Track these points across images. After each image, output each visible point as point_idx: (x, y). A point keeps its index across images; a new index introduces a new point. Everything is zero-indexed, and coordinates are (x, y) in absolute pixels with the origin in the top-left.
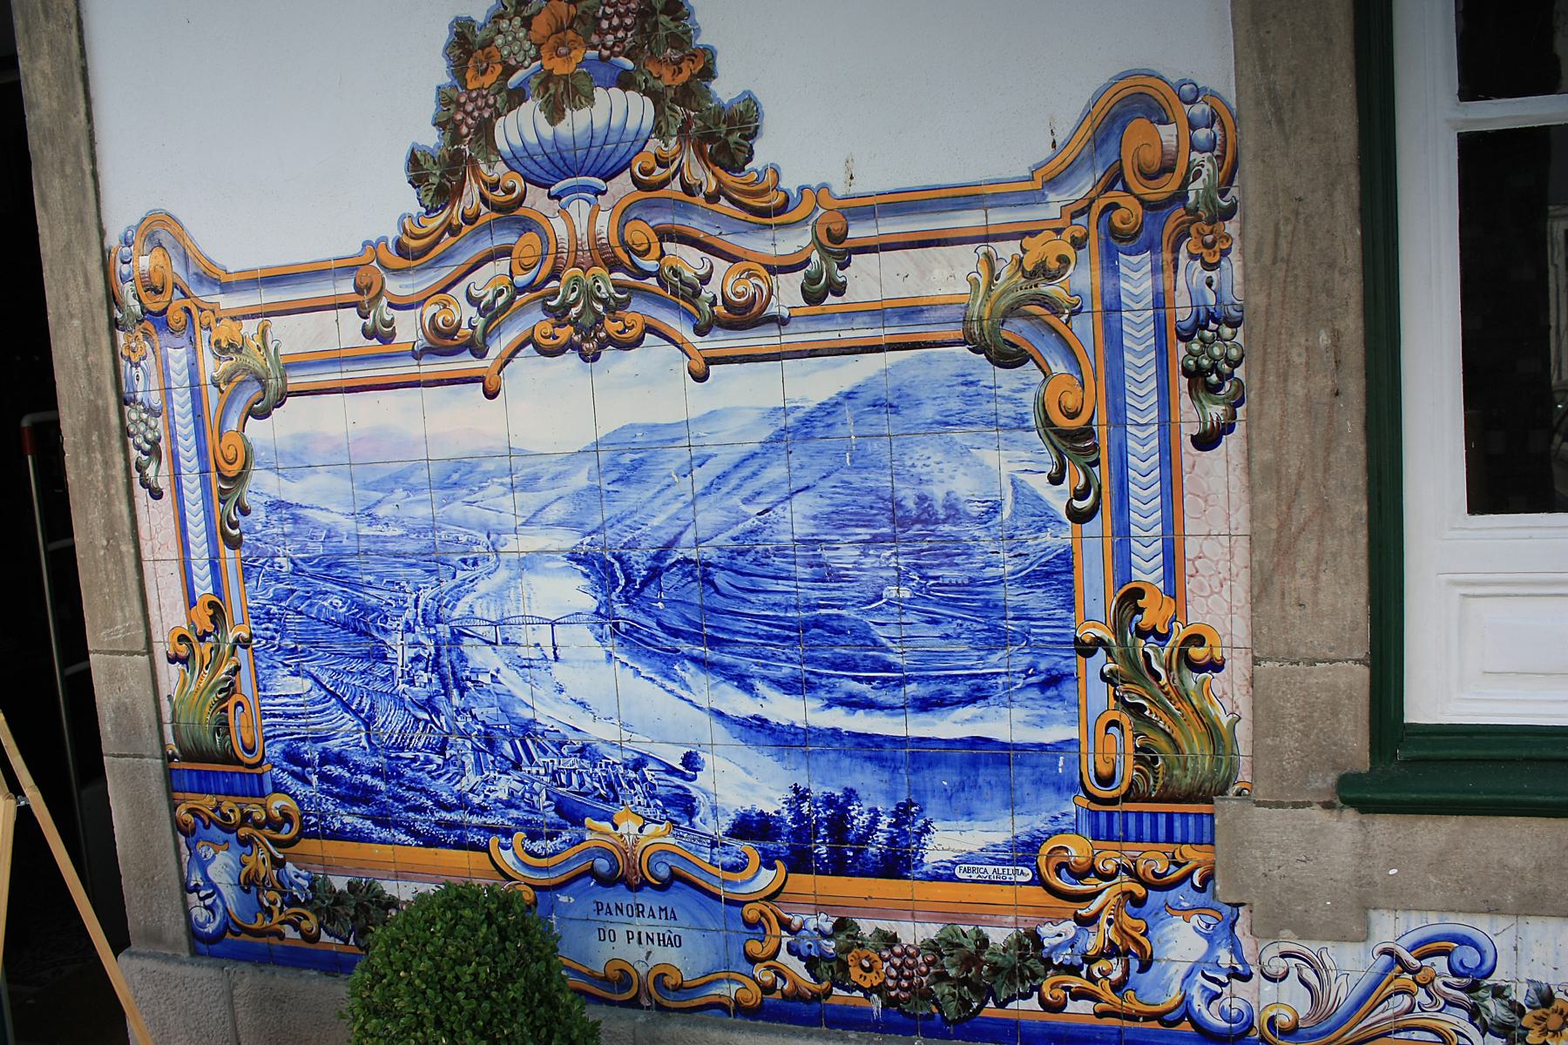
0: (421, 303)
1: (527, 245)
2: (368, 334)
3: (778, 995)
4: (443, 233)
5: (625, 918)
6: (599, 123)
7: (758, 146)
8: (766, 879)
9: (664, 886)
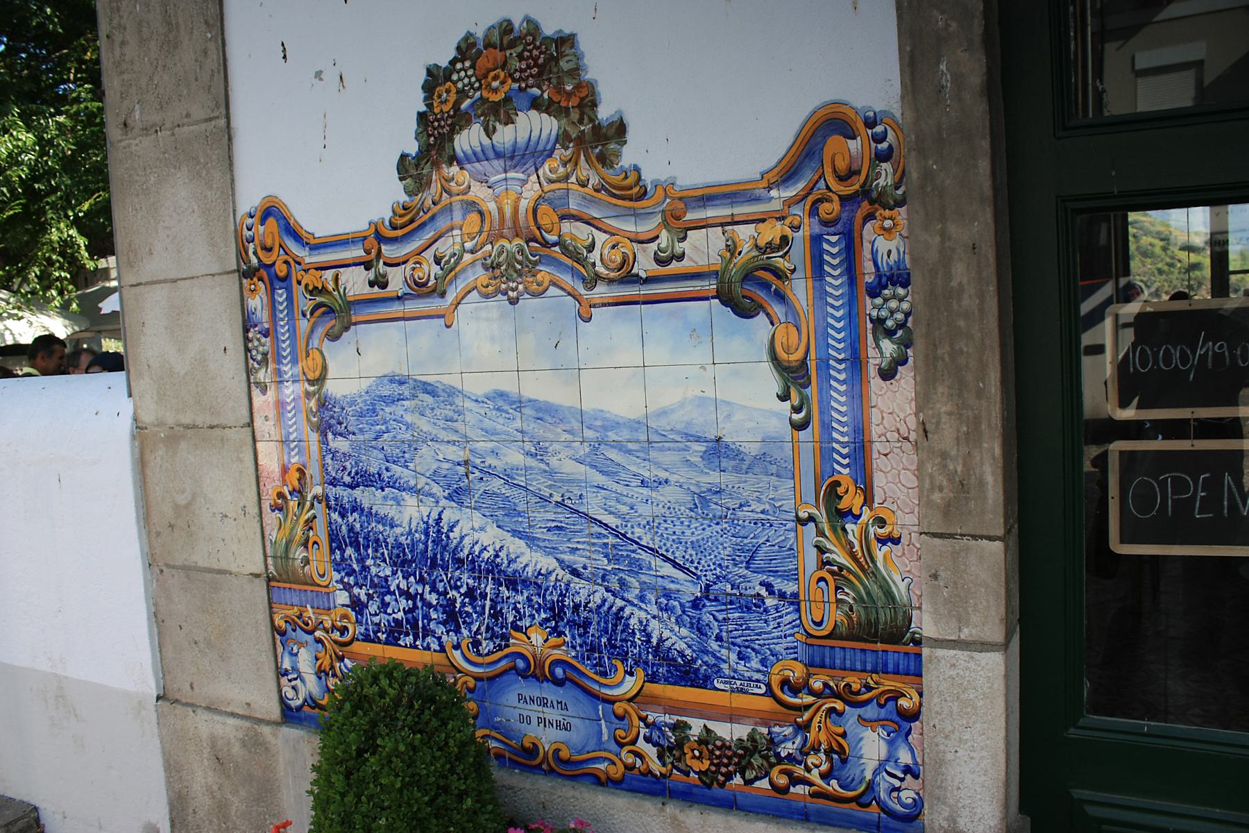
0: (404, 263)
2: (372, 284)
3: (635, 772)
5: (535, 707)
8: (630, 685)
9: (559, 683)
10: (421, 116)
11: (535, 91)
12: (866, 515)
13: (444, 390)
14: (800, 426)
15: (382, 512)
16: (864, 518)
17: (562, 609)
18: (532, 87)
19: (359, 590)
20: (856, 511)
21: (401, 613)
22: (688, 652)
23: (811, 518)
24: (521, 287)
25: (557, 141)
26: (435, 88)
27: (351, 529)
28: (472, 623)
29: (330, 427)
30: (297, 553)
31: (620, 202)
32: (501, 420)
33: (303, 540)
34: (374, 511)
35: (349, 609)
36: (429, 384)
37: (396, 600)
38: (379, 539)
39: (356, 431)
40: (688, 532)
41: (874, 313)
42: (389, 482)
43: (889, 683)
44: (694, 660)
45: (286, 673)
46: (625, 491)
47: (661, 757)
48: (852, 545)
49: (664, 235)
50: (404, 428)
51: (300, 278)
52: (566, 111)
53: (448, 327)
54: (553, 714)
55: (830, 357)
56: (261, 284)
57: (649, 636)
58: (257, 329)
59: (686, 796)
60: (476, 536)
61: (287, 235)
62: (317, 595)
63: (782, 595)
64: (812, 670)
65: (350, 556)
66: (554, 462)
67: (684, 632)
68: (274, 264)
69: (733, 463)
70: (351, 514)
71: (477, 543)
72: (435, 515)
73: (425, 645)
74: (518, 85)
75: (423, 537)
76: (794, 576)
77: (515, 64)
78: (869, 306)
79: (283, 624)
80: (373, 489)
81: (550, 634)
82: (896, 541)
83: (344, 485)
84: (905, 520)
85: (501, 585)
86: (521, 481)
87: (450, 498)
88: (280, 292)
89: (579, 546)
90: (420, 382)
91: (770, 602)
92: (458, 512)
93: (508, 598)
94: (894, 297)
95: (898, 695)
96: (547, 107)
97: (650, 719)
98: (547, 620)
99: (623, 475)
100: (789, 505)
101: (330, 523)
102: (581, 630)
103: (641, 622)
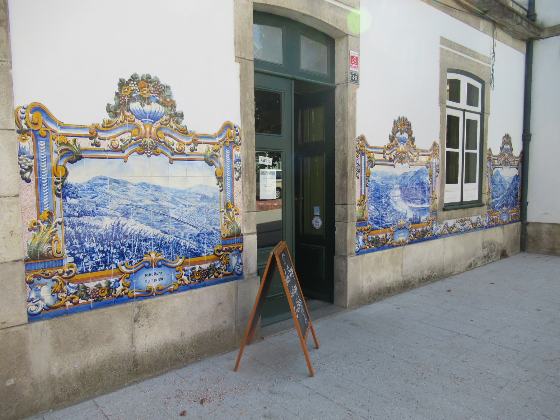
1: (136, 131)
2: (92, 145)
3: (182, 285)
4: (115, 124)
6: (153, 110)
7: (183, 121)
8: (181, 261)
9: (160, 267)
10: (117, 94)
11: (158, 98)
12: (233, 209)
13: (122, 182)
14: (221, 191)
15: (93, 224)
16: (233, 210)
17: (161, 245)
18: (157, 96)
19: (79, 255)
20: (231, 209)
21: (100, 259)
22: (196, 248)
23: (223, 211)
24: (152, 153)
25: (164, 114)
26: (123, 86)
27: (77, 232)
28: (130, 255)
29: (68, 195)
30: (45, 247)
31: (182, 134)
32: (144, 191)
33: (48, 241)
34: (89, 224)
35: (74, 263)
36: (117, 180)
37: (98, 255)
38: (91, 234)
39: (82, 196)
40: (196, 218)
41: (235, 167)
42: (97, 214)
43: (237, 246)
44: (197, 250)
45: (32, 299)
46: (180, 209)
47: (188, 279)
48: (230, 216)
49: (192, 144)
50: (105, 194)
51: (54, 138)
52: (168, 107)
53: (125, 162)
54: (157, 277)
55: (227, 175)
56: (29, 137)
57: (186, 246)
58: (26, 155)
59: (195, 287)
60: (133, 227)
61: (47, 120)
62: (55, 262)
63: (217, 230)
64: (223, 246)
65: (76, 243)
66: (160, 202)
67: (195, 243)
68: (39, 130)
69: (207, 200)
70: (78, 227)
71: (133, 229)
72: (117, 222)
73: (110, 268)
74: (152, 94)
75: (111, 231)
76: (219, 225)
77: (152, 89)
78: (234, 165)
79: (32, 279)
80: (90, 217)
81: (157, 252)
82: (238, 214)
83: (75, 216)
84: (240, 210)
85: (141, 241)
86: (150, 208)
87: (123, 216)
88: (42, 142)
89: (167, 225)
90: (113, 179)
91: (215, 232)
92: (126, 221)
93: (144, 245)
94: (238, 164)
95: (239, 247)
96: (162, 104)
97: (186, 269)
98: (157, 249)
99: (180, 205)
100: (218, 209)
101: (66, 232)
102: (167, 249)
103: (184, 243)
